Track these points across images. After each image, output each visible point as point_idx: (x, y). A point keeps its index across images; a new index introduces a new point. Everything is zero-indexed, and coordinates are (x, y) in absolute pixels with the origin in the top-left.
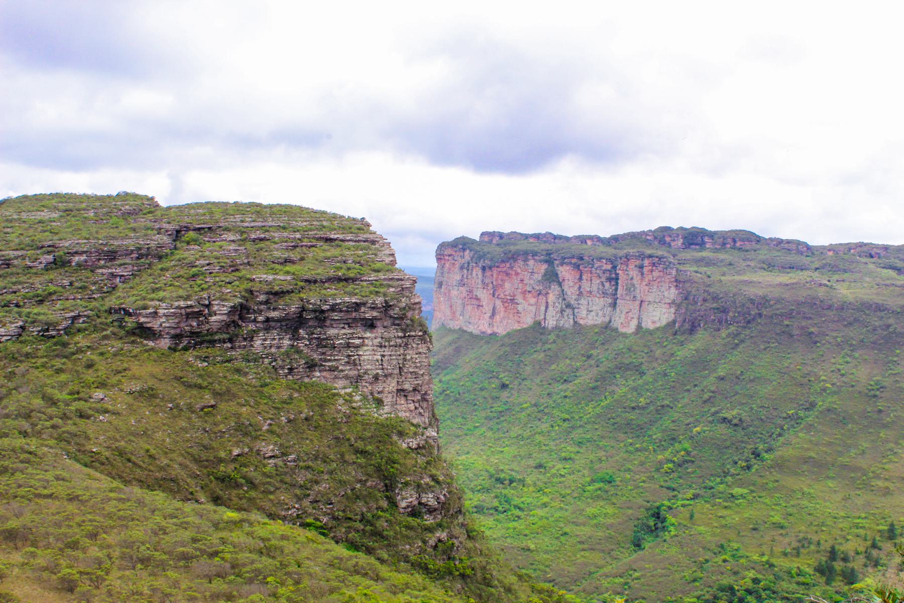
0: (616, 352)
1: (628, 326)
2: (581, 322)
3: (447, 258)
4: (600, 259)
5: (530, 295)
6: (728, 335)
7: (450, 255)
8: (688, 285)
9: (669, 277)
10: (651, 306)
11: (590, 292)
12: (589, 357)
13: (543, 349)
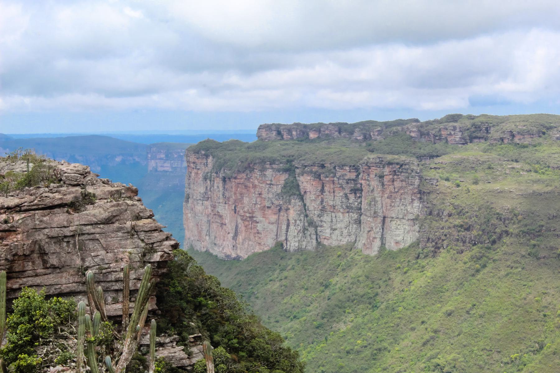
0: (350, 281)
1: (371, 248)
2: (326, 242)
3: (192, 165)
4: (342, 166)
5: (270, 211)
6: (472, 258)
7: (194, 163)
8: (432, 196)
9: (411, 187)
10: (394, 223)
11: (334, 207)
12: (326, 287)
13: (279, 278)
